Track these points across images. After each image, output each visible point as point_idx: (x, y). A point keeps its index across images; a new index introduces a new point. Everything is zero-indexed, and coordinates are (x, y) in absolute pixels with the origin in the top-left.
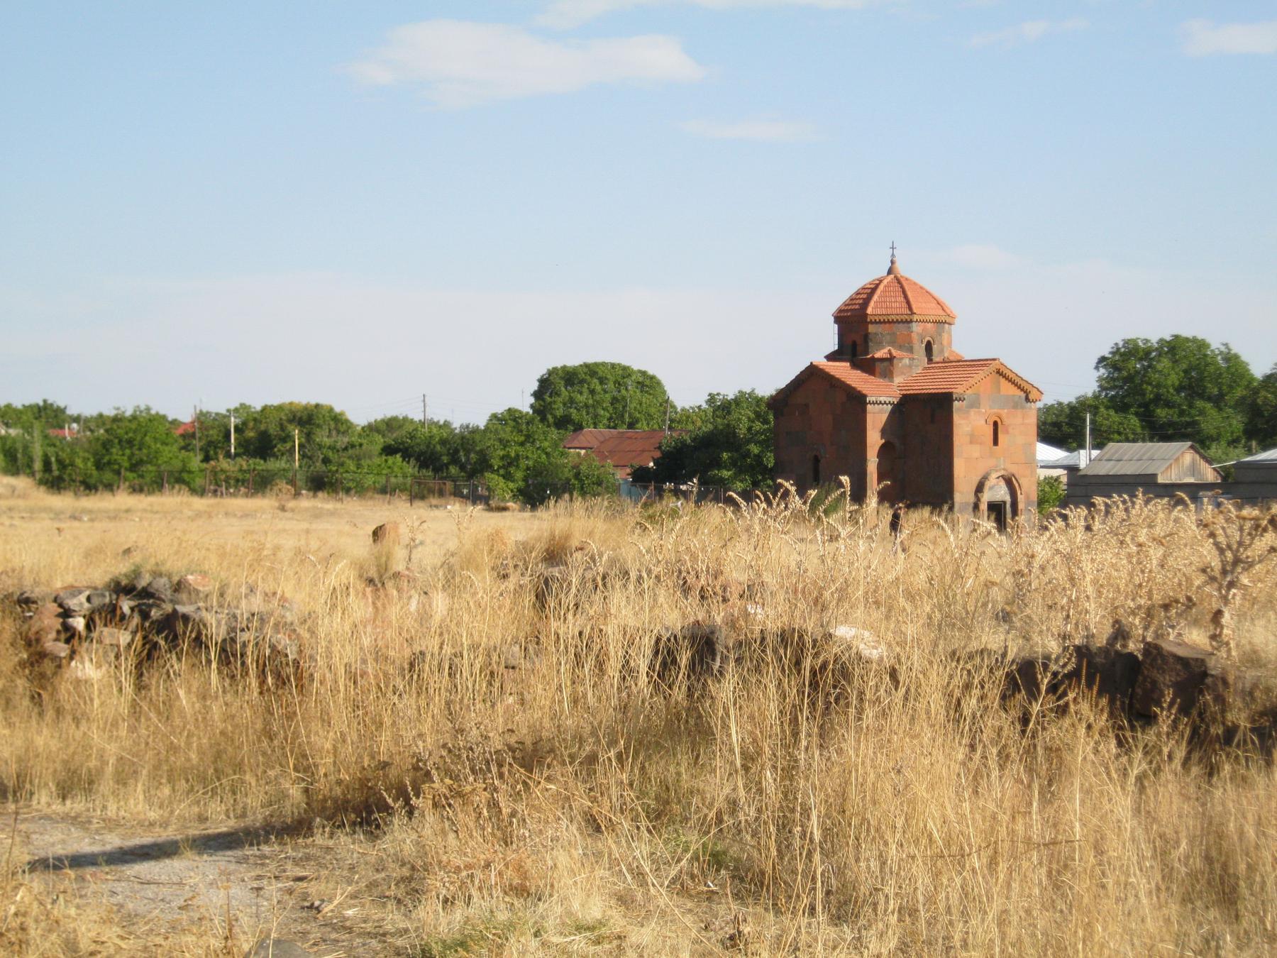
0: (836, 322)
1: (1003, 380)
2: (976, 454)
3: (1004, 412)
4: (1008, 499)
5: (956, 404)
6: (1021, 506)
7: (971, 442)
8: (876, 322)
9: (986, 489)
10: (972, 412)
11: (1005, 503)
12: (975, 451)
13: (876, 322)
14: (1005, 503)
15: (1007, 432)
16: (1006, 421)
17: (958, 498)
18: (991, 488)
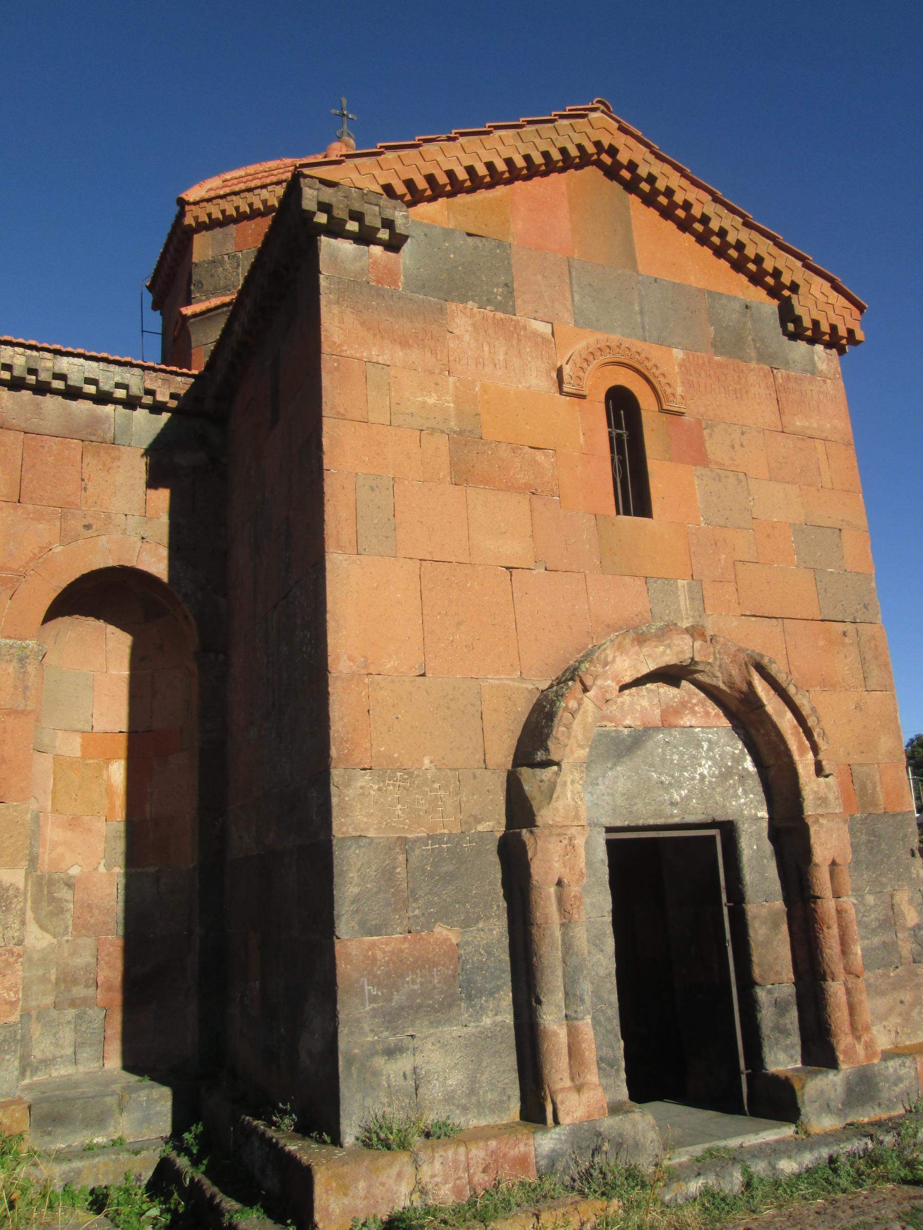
0: (155, 307)
1: (644, 218)
2: (514, 549)
3: (670, 361)
4: (750, 809)
5: (336, 252)
6: (828, 842)
7: (462, 475)
8: (213, 224)
9: (572, 740)
10: (463, 320)
11: (728, 829)
12: (498, 529)
13: (213, 224)
14: (728, 829)
15: (700, 458)
16: (677, 390)
17: (364, 810)
18: (623, 746)
